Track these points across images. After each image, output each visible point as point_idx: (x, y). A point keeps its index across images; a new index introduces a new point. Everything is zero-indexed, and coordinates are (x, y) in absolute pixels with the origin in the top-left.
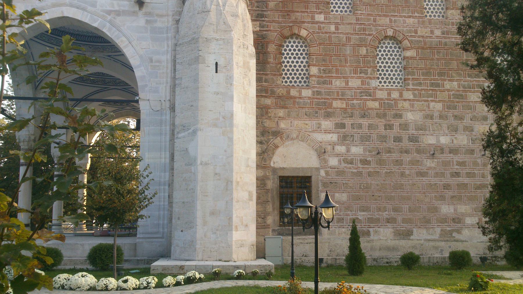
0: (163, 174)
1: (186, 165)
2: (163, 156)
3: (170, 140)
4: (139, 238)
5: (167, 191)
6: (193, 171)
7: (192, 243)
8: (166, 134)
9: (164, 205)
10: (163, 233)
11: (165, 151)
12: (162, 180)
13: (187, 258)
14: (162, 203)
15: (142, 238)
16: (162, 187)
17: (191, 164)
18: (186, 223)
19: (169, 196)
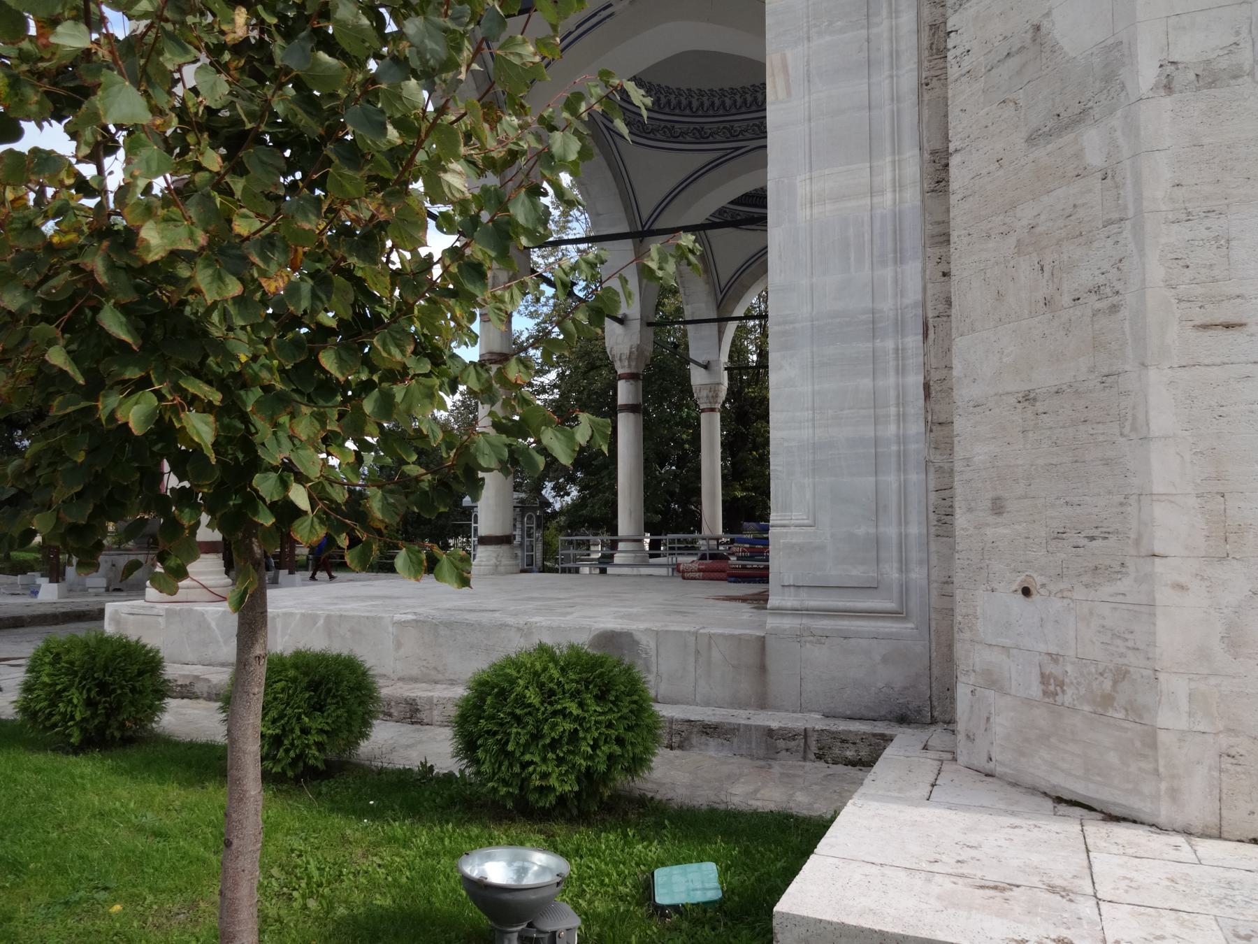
0: (888, 273)
1: (1031, 140)
2: (888, 176)
3: (924, 84)
4: (780, 611)
5: (914, 360)
6: (1095, 159)
7: (1119, 693)
8: (895, 55)
9: (902, 440)
10: (905, 591)
11: (897, 149)
12: (887, 306)
13: (1079, 789)
14: (892, 429)
15: (796, 612)
16: (890, 344)
17: (1081, 117)
18: (1059, 536)
19: (927, 387)
